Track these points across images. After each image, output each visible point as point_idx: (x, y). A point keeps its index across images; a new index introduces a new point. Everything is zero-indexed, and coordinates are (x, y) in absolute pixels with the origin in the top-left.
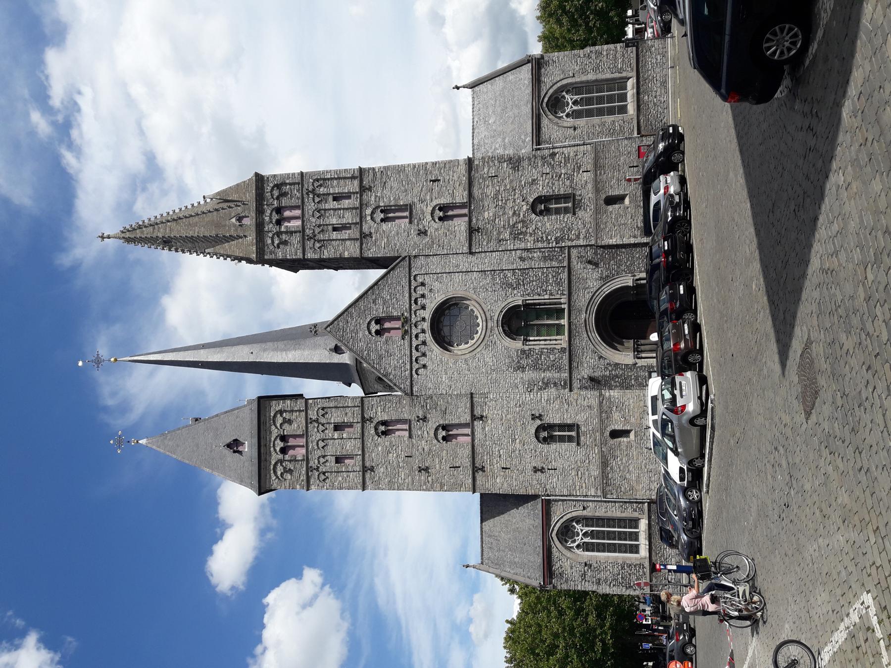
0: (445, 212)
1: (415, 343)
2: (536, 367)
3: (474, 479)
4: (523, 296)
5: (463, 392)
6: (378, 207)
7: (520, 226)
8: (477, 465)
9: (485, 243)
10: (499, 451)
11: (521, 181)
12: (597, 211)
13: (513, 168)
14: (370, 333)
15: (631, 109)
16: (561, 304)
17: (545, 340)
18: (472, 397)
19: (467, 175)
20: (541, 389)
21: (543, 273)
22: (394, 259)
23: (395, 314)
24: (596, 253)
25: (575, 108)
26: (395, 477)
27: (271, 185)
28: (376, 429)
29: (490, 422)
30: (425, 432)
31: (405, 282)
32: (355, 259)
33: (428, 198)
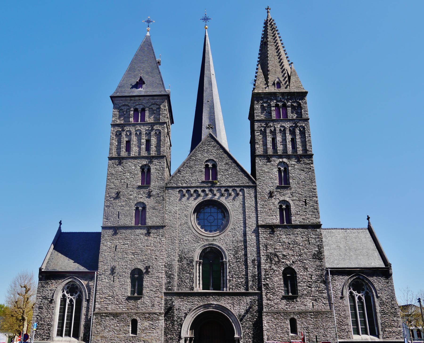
0: (285, 210)
2: (182, 269)
6: (288, 167)
9: (264, 235)
11: (306, 260)
12: (286, 313)
13: (314, 255)
15: (356, 338)
17: (199, 276)
19: (310, 223)
20: (166, 272)
25: (356, 298)
26: (114, 177)
29: (146, 238)
30: (141, 196)
31: (240, 183)
32: (255, 153)
33: (295, 198)
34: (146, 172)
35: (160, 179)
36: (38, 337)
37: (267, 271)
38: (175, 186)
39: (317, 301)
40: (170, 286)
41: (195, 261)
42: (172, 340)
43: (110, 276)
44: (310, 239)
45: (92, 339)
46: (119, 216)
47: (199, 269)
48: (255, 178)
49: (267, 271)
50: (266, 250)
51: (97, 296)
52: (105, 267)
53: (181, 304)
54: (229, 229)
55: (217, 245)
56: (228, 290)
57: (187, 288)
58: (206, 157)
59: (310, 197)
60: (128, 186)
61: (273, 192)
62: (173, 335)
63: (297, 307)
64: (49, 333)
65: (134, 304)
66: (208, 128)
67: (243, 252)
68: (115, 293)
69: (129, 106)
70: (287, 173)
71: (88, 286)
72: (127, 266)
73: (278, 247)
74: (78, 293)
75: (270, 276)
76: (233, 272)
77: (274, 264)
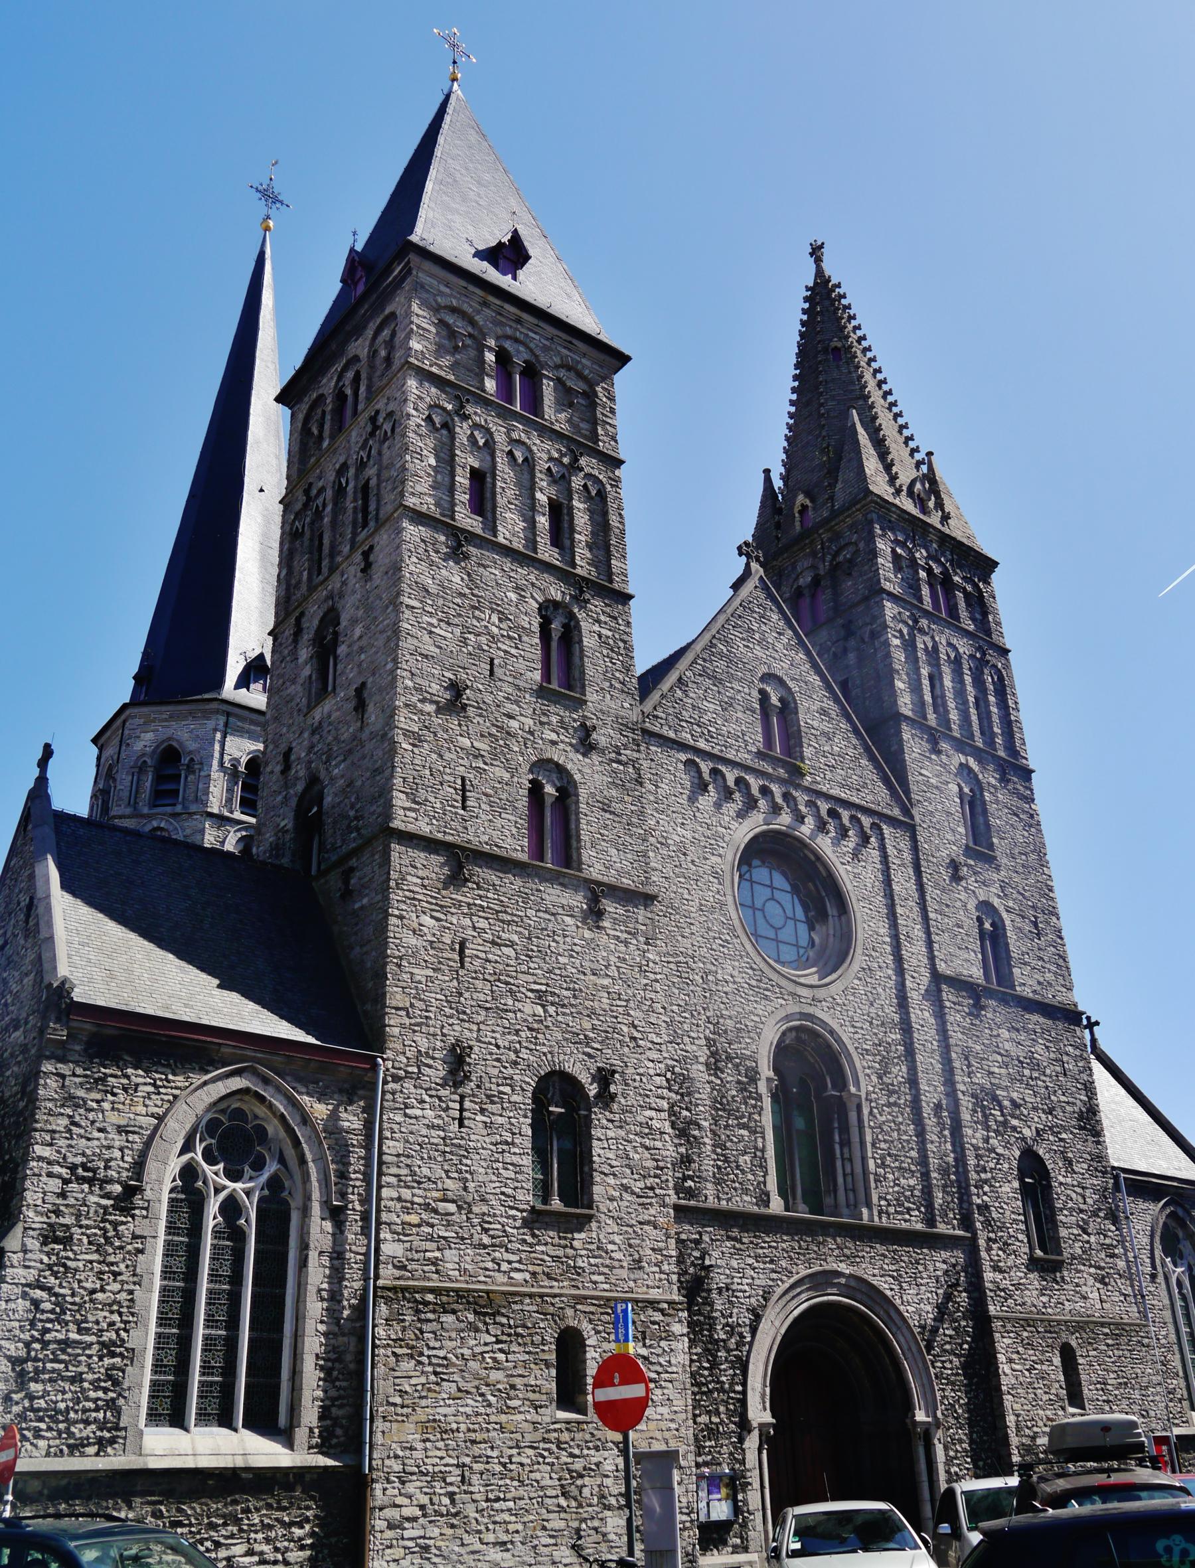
2: (720, 1105)
3: (429, 845)
10: (512, 944)
30: (554, 737)
35: (617, 685)
36: (37, 1434)
38: (672, 735)
40: (691, 1178)
41: (763, 1077)
42: (717, 1440)
43: (442, 1093)
45: (379, 1439)
46: (464, 799)
51: (385, 1192)
53: (734, 1264)
54: (856, 967)
55: (824, 1024)
56: (876, 1219)
57: (746, 1191)
60: (499, 672)
62: (718, 1413)
64: (111, 1405)
65: (560, 1253)
67: (904, 1069)
68: (471, 1185)
71: (333, 1128)
74: (271, 1168)
75: (989, 1175)
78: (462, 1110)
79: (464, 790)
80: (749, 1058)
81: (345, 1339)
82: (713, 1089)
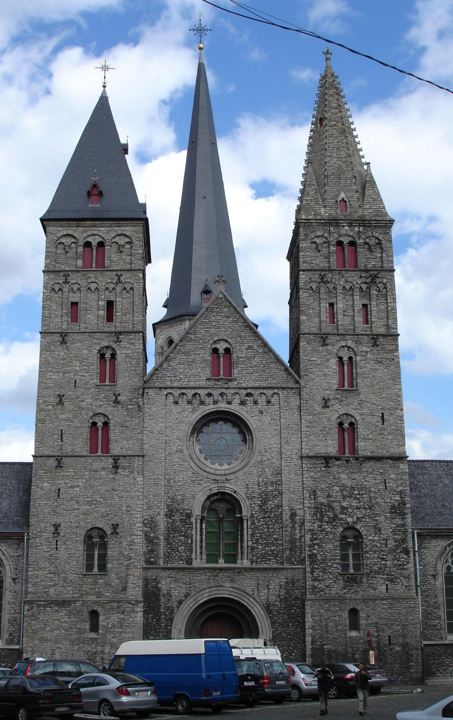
0: (347, 430)
1: (201, 392)
2: (171, 529)
4: (252, 516)
5: (146, 447)
6: (356, 355)
7: (331, 514)
8: (63, 461)
9: (312, 474)
10: (78, 486)
11: (379, 515)
13: (393, 507)
14: (215, 342)
16: (242, 559)
18: (139, 456)
19: (388, 455)
20: (146, 534)
21: (276, 539)
22: (298, 372)
23: (235, 371)
24: (296, 599)
27: (381, 237)
28: (107, 347)
30: (101, 403)
31: (272, 382)
32: (298, 327)
34: (107, 360)
37: (315, 534)
39: (394, 582)
41: (194, 515)
44: (387, 481)
47: (201, 528)
48: (299, 376)
49: (315, 534)
50: (314, 500)
52: (41, 524)
57: (181, 560)
58: (212, 336)
59: (390, 410)
61: (329, 399)
63: (361, 593)
66: (218, 281)
69: (74, 237)
70: (354, 366)
72: (79, 523)
73: (334, 494)
75: (319, 541)
76: (258, 535)
77: (326, 522)
78: (57, 545)
79: (62, 435)
80: (188, 509)
81: (17, 615)
82: (168, 524)
